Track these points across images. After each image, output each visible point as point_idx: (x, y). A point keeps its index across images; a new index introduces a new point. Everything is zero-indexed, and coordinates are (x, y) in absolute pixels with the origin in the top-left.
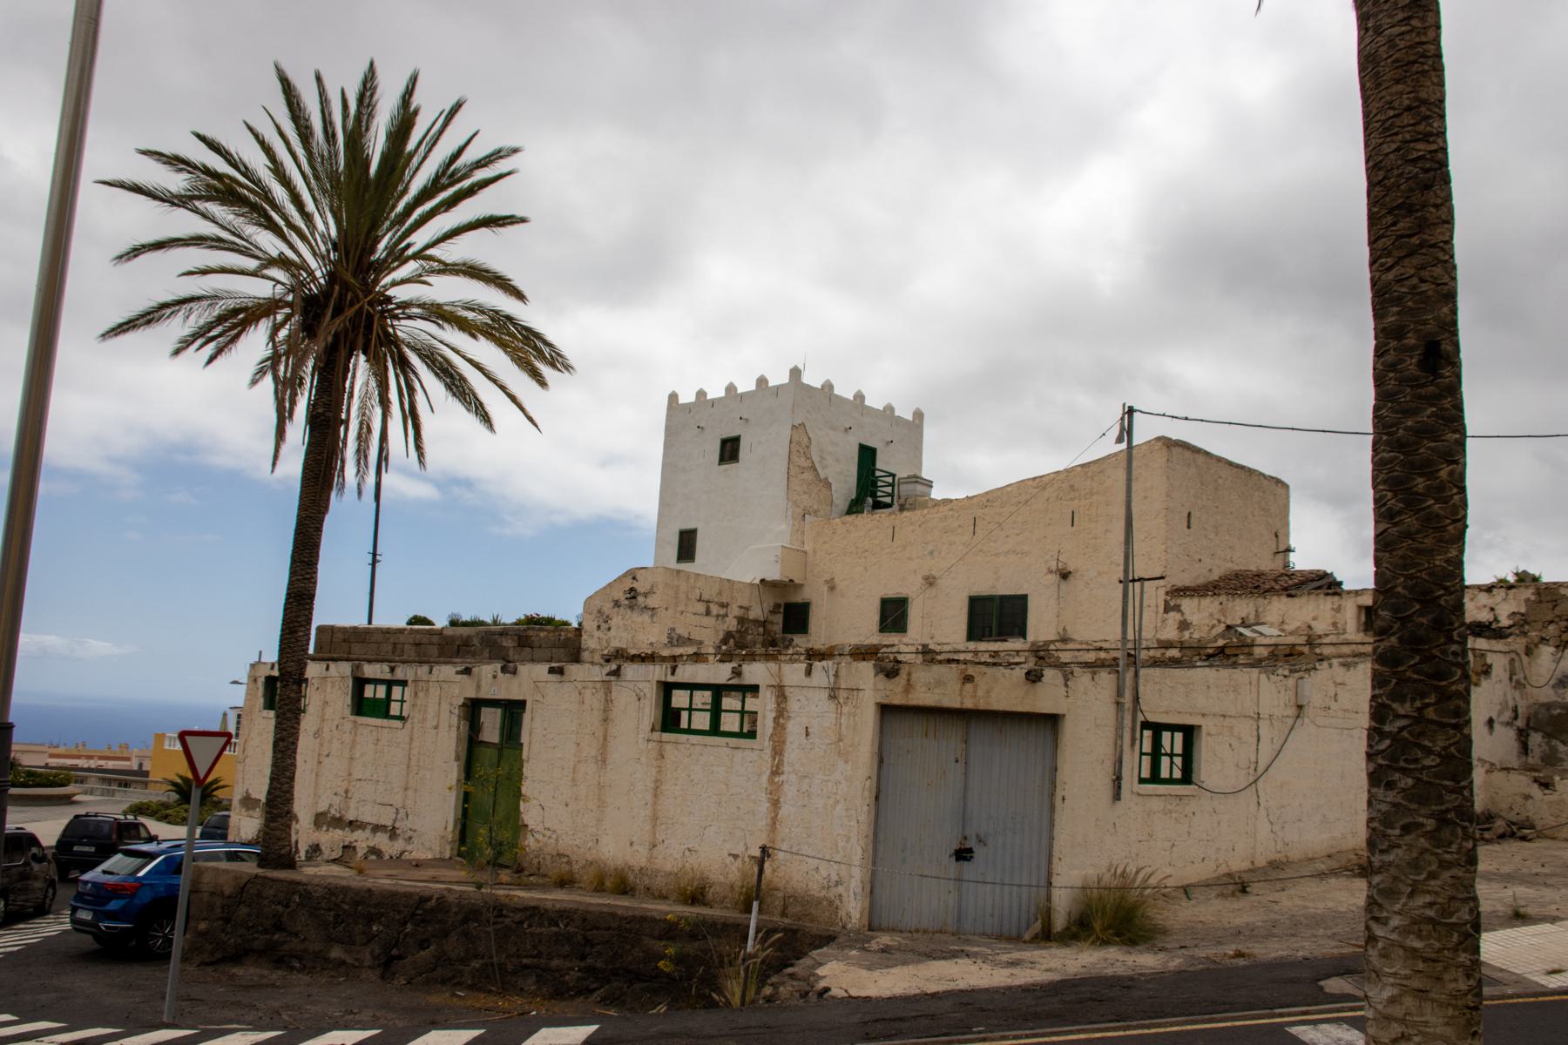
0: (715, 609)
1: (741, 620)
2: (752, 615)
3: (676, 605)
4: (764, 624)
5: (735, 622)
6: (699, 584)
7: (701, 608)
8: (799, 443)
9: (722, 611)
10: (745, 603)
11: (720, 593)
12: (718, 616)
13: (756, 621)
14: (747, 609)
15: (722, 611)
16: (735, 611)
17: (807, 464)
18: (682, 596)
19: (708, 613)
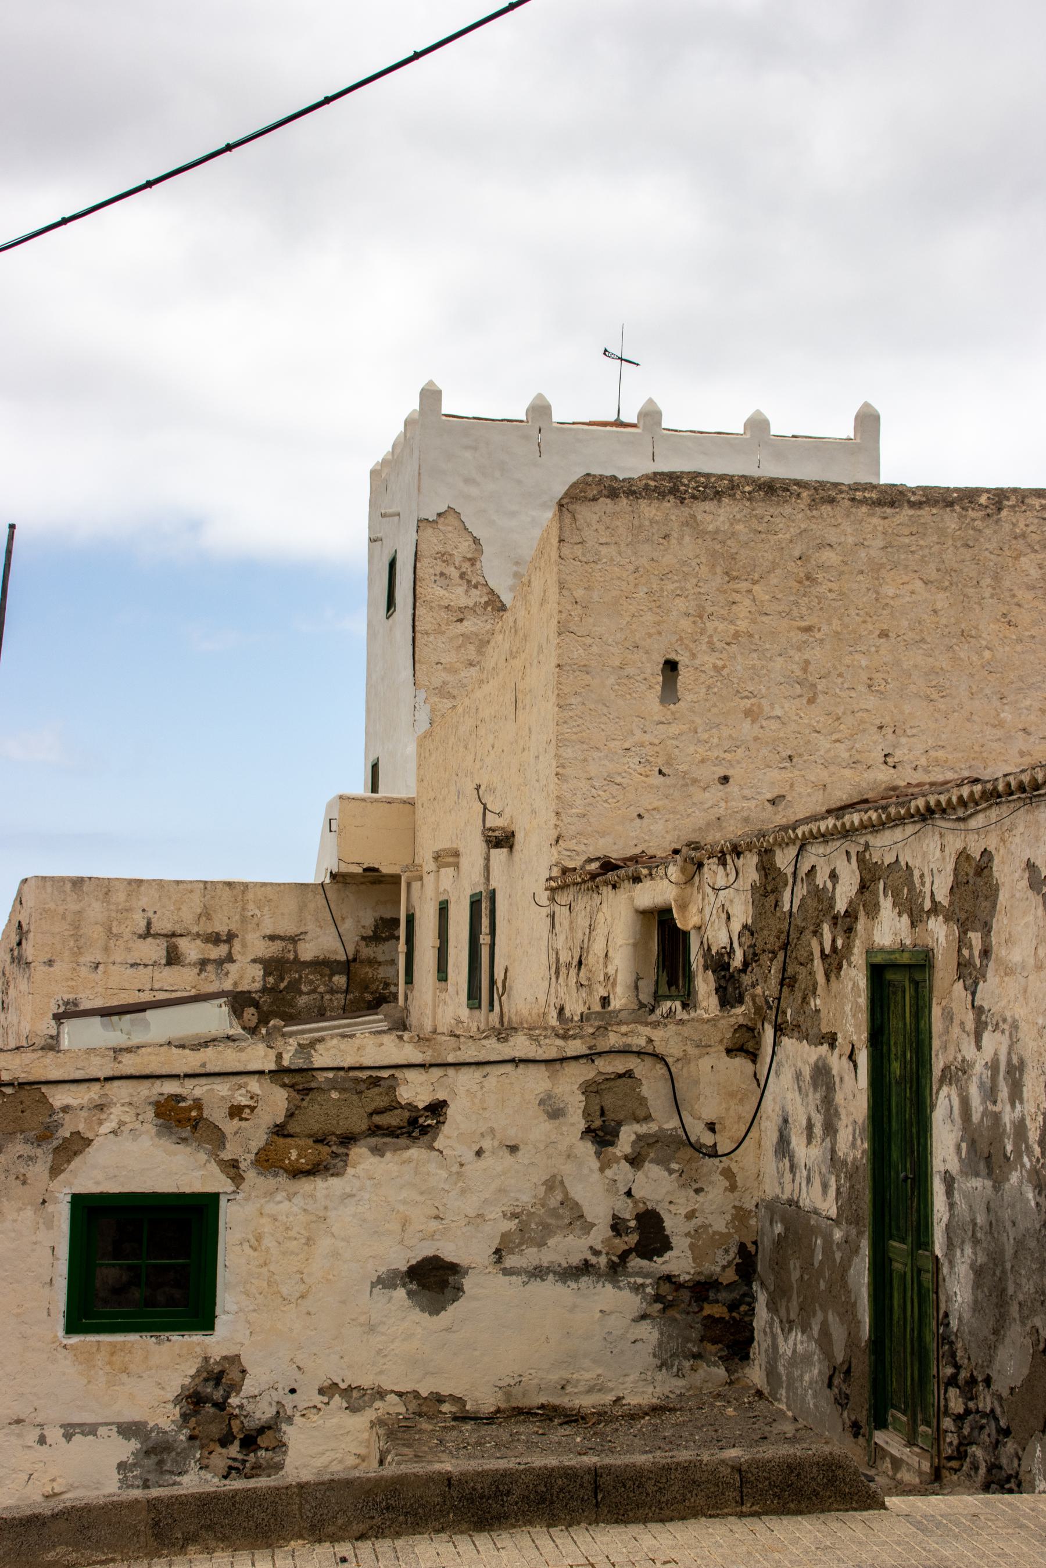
0: (191, 950)
1: (272, 966)
2: (308, 952)
3: (78, 951)
4: (347, 967)
5: (258, 971)
6: (144, 902)
7: (154, 950)
8: (444, 557)
9: (222, 950)
10: (286, 927)
11: (206, 914)
12: (203, 963)
13: (323, 965)
14: (294, 940)
15: (217, 952)
16: (255, 946)
17: (479, 596)
18: (95, 933)
19: (173, 958)
